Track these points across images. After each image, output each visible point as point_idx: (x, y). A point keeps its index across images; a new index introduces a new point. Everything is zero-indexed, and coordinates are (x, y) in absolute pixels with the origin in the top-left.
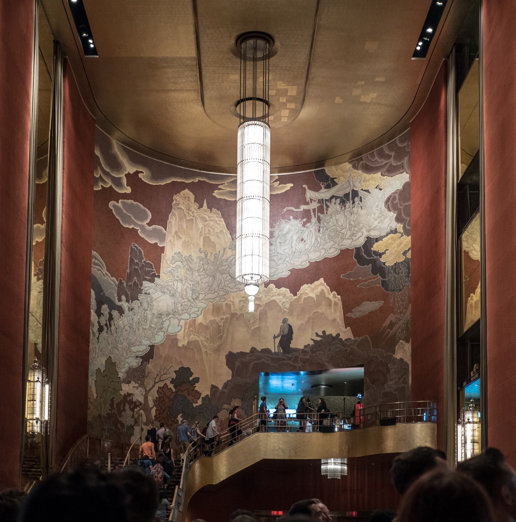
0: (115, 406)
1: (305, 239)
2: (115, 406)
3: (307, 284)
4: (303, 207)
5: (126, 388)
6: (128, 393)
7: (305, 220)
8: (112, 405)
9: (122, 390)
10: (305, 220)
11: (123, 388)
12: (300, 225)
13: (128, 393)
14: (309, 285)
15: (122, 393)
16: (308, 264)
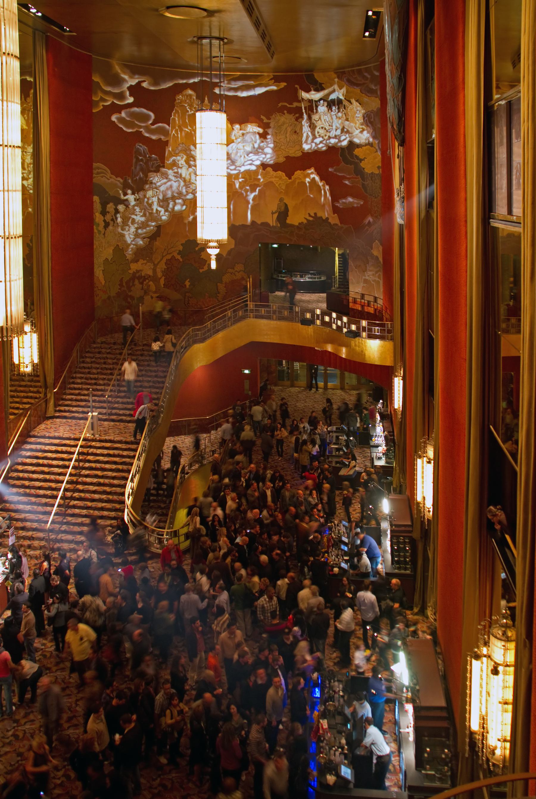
0: (124, 284)
1: (298, 131)
2: (124, 284)
3: (300, 170)
4: (295, 104)
5: (134, 267)
6: (136, 270)
7: (297, 115)
8: (121, 285)
9: (130, 269)
10: (297, 115)
11: (132, 267)
12: (293, 120)
13: (136, 270)
14: (302, 171)
15: (131, 272)
16: (300, 154)
